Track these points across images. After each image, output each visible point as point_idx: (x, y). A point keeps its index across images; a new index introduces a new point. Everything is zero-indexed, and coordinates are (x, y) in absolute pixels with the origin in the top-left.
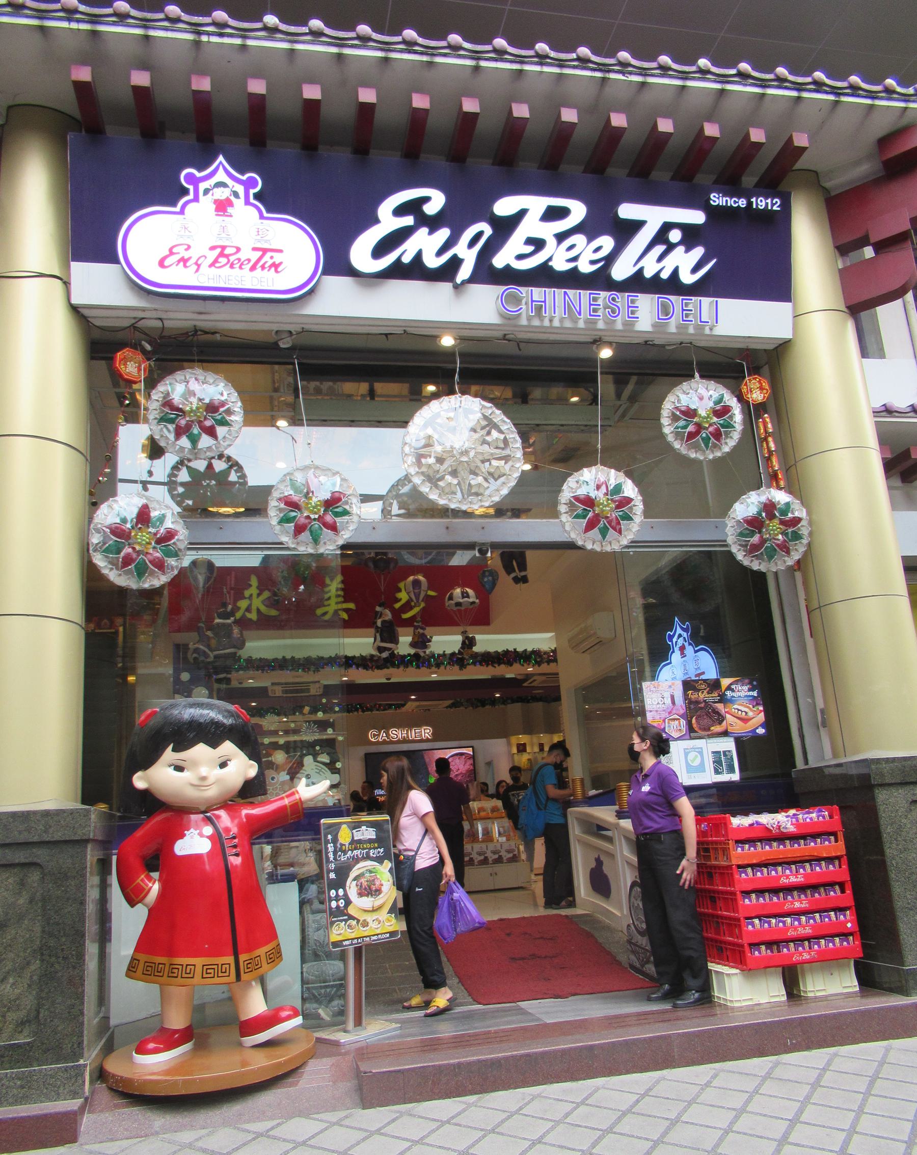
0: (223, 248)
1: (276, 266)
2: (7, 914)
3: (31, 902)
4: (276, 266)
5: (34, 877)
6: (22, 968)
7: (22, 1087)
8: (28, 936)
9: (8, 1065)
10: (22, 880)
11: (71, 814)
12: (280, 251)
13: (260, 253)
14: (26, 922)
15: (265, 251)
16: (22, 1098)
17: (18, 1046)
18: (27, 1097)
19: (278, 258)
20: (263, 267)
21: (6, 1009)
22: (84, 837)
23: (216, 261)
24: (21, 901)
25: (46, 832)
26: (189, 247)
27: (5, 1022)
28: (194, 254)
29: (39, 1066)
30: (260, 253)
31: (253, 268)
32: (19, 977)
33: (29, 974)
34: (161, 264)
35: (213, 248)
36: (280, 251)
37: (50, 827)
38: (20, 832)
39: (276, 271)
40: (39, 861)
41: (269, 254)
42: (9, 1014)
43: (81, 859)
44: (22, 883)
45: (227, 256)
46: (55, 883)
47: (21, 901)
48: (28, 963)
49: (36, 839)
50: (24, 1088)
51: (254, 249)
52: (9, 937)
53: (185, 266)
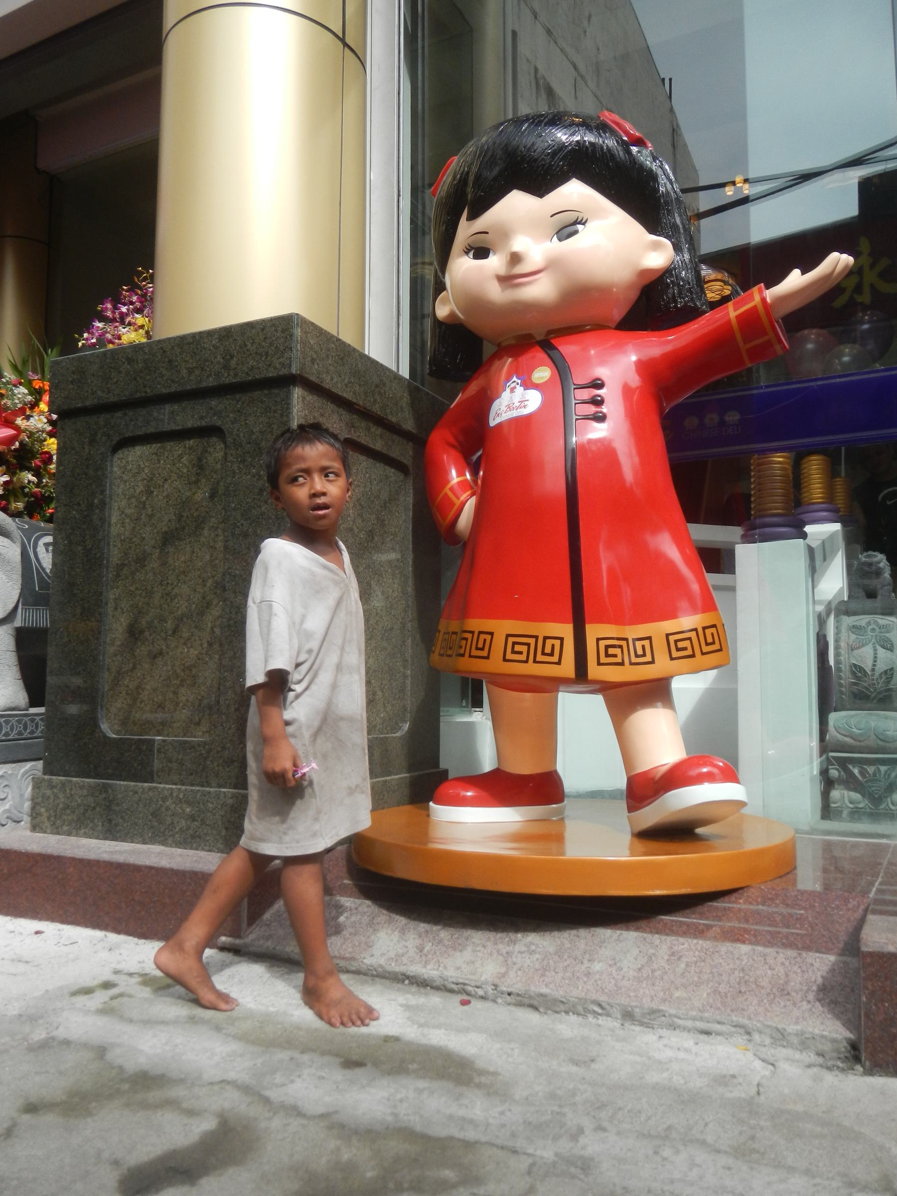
2: (180, 517)
3: (212, 496)
5: (216, 451)
6: (202, 614)
7: (193, 818)
8: (208, 557)
9: (175, 778)
10: (200, 459)
11: (263, 330)
14: (206, 532)
16: (193, 837)
17: (192, 746)
18: (200, 837)
21: (177, 682)
22: (284, 372)
24: (199, 496)
25: (226, 367)
27: (177, 704)
29: (220, 786)
32: (196, 627)
33: (210, 625)
37: (232, 357)
38: (191, 371)
40: (219, 423)
42: (183, 690)
43: (282, 415)
44: (200, 466)
46: (243, 461)
47: (199, 496)
48: (209, 605)
49: (211, 382)
50: (194, 820)
52: (183, 559)
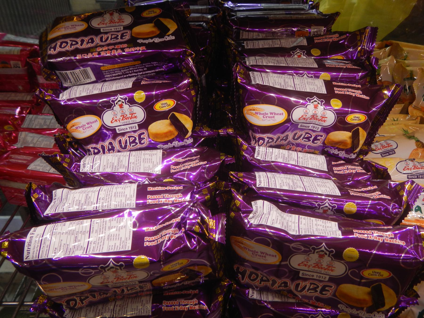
0: (123, 115)
1: (136, 117)
4: (136, 117)
12: (135, 113)
13: (131, 115)
15: (132, 114)
19: (135, 115)
20: (133, 118)
23: (123, 119)
26: (116, 117)
28: (118, 118)
30: (131, 115)
31: (131, 119)
34: (112, 122)
35: (121, 116)
36: (135, 113)
39: (136, 118)
41: (133, 115)
45: (125, 117)
51: (130, 114)
53: (117, 121)
